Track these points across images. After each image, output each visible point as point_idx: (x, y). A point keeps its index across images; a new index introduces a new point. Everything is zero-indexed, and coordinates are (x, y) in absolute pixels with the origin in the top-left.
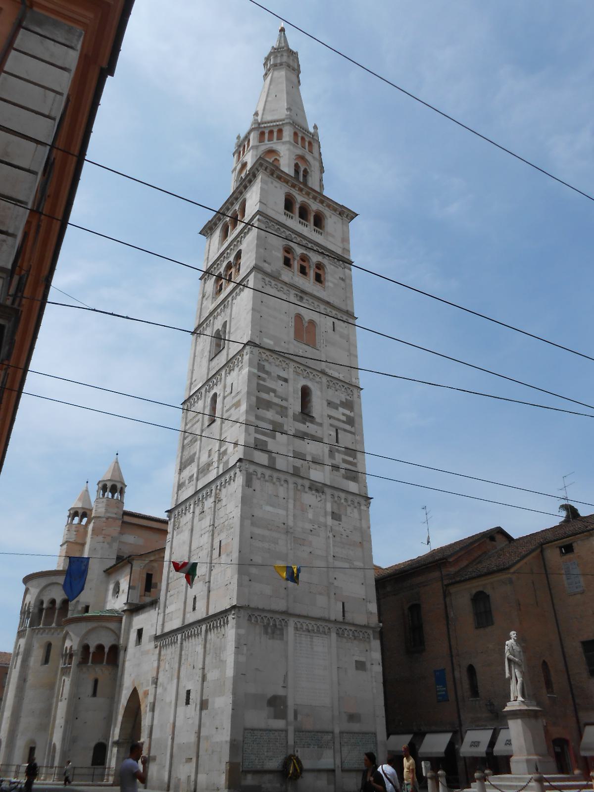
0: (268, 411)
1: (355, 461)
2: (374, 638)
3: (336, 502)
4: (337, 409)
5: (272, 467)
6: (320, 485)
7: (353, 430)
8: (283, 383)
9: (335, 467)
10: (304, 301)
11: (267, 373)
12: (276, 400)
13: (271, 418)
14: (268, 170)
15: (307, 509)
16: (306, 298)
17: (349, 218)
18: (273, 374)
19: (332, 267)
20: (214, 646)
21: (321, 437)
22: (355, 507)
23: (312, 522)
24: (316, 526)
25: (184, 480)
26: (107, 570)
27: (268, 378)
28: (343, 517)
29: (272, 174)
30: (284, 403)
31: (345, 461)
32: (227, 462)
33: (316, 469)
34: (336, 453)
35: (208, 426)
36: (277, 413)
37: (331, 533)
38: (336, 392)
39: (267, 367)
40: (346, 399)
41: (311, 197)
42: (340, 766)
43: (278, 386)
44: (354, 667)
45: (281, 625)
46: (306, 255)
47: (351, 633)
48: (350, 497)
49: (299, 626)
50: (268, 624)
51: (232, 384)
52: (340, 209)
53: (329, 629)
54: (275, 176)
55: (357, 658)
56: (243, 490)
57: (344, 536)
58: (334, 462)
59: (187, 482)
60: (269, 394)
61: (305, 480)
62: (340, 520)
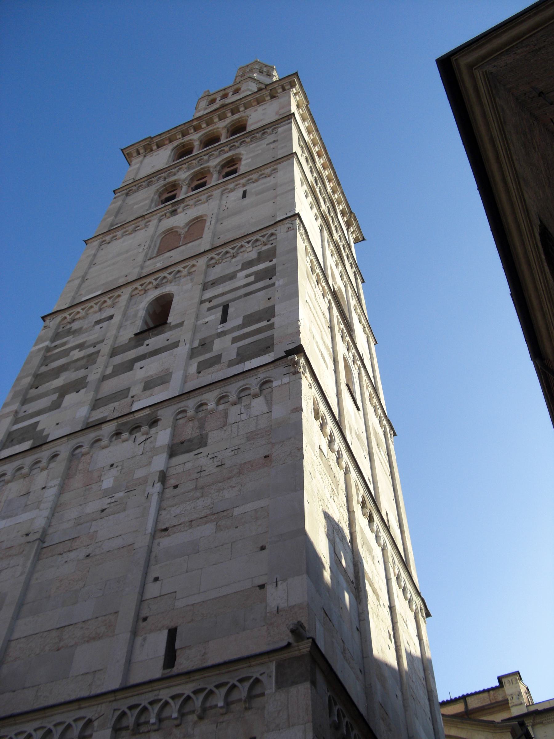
3: (191, 419)
6: (147, 412)
10: (179, 211)
14: (142, 151)
15: (100, 477)
16: (182, 205)
17: (287, 88)
22: (255, 396)
27: (73, 337)
28: (214, 437)
29: (152, 150)
38: (234, 260)
41: (216, 120)
46: (202, 169)
52: (267, 93)
54: (155, 147)
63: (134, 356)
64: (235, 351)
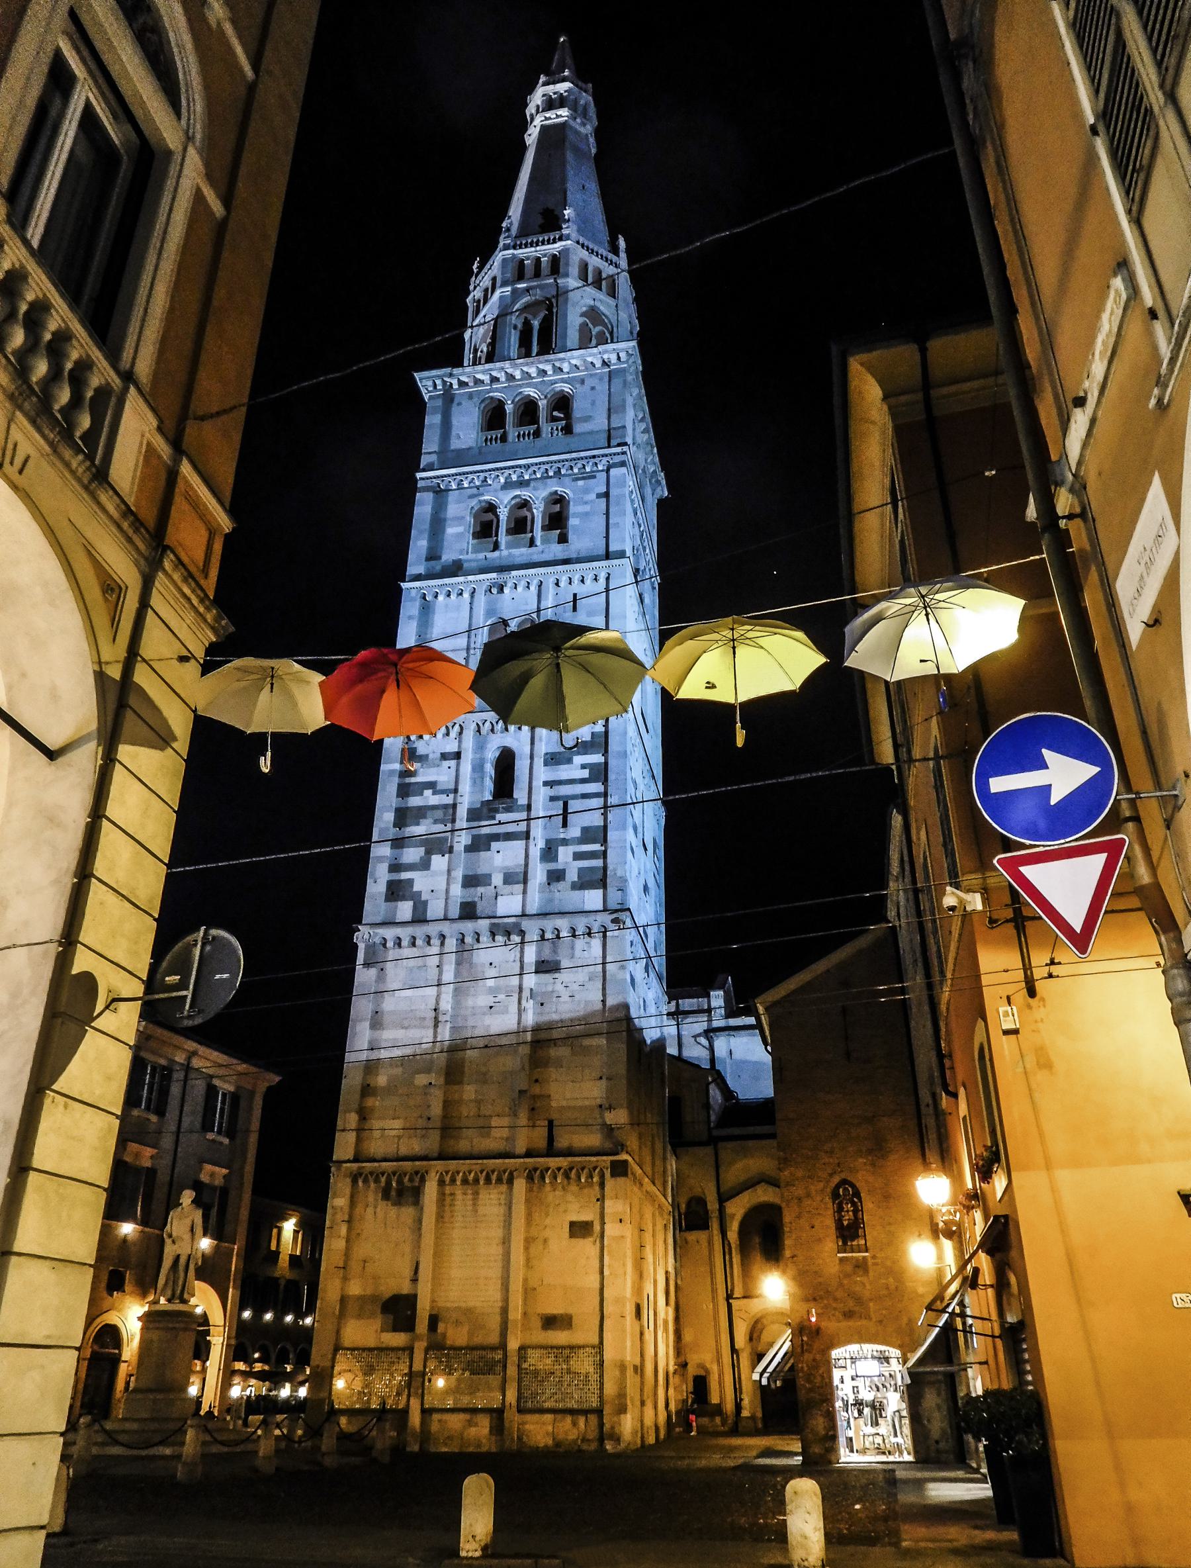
2: (613, 1175)
5: (420, 918)
8: (453, 763)
9: (555, 876)
18: (431, 756)
19: (581, 483)
31: (578, 856)
34: (561, 849)
36: (436, 822)
37: (531, 1002)
42: (514, 1403)
44: (568, 1235)
48: (581, 924)
55: (575, 1218)
57: (565, 997)
58: (552, 866)
60: (422, 794)
61: (480, 922)
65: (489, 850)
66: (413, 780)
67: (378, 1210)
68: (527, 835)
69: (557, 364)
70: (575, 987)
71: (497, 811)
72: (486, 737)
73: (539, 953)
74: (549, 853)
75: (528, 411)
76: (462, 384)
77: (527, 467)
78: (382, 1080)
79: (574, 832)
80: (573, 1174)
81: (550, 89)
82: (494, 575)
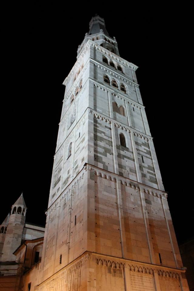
0: (101, 142)
1: (154, 173)
4: (141, 146)
6: (136, 183)
7: (150, 157)
9: (144, 176)
11: (99, 124)
12: (105, 137)
13: (103, 146)
18: (102, 125)
20: (73, 284)
21: (133, 158)
22: (159, 197)
23: (133, 203)
24: (136, 206)
25: (55, 192)
26: (15, 252)
27: (100, 126)
28: (152, 202)
30: (110, 139)
31: (148, 172)
32: (79, 170)
33: (132, 175)
35: (67, 159)
36: (107, 144)
37: (146, 211)
39: (99, 121)
40: (145, 142)
43: (107, 131)
45: (120, 267)
47: (167, 274)
48: (155, 192)
49: (132, 268)
50: (111, 266)
51: (80, 133)
53: (153, 271)
56: (88, 181)
58: (143, 172)
59: (56, 192)
60: (101, 134)
61: (127, 180)
62: (151, 204)
63: (123, 154)
64: (149, 177)
65: (124, 159)
66: (98, 128)
67: (107, 277)
68: (134, 160)
69: (121, 60)
70: (156, 211)
71: (124, 150)
72: (117, 128)
73: (145, 197)
74: (141, 167)
75: (112, 64)
76: (98, 49)
77: (117, 75)
78: (101, 223)
79: (146, 166)
80: (171, 275)
81: (100, 18)
82: (114, 91)
